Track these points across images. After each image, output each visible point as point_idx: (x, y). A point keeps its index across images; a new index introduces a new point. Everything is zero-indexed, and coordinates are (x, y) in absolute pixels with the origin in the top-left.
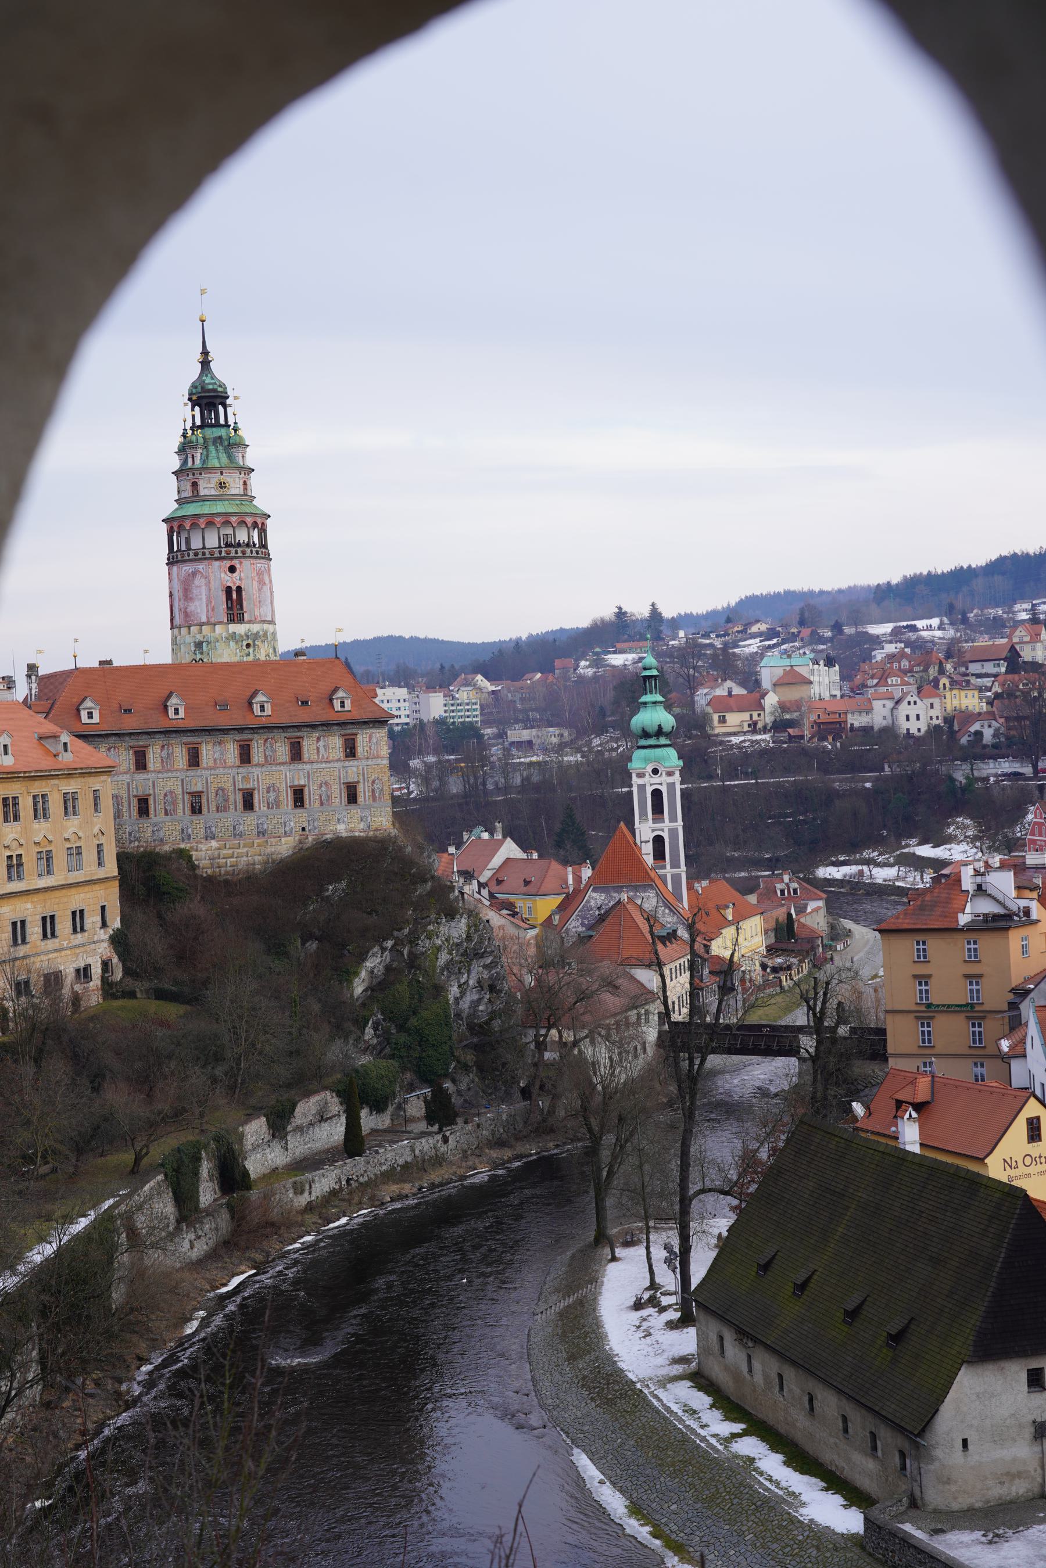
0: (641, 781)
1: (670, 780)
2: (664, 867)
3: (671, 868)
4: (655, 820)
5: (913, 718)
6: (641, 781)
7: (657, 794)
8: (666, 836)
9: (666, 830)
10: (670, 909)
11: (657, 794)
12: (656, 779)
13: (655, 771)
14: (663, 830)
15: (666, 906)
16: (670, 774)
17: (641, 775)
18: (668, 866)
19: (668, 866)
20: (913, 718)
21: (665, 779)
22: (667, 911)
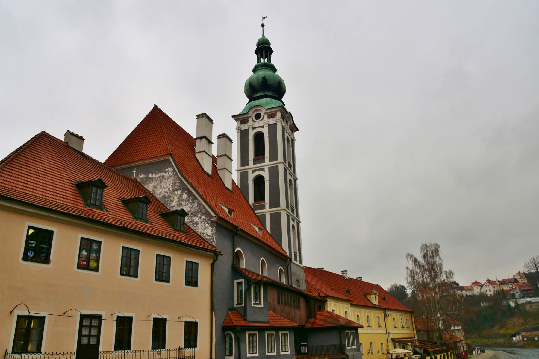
0: (244, 127)
1: (272, 121)
2: (264, 208)
3: (271, 207)
4: (255, 161)
5: (488, 291)
6: (244, 127)
7: (259, 137)
8: (266, 174)
9: (267, 169)
10: (190, 194)
11: (259, 137)
12: (259, 123)
13: (258, 116)
15: (184, 189)
18: (267, 206)
19: (267, 206)
20: (488, 291)
21: (267, 120)
22: (185, 196)
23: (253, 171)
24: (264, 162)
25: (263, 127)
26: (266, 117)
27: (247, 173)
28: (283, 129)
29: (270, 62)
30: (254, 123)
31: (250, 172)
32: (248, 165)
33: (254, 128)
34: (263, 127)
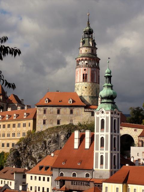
0: (98, 116)
6: (98, 116)
12: (103, 115)
13: (103, 112)
14: (104, 135)
16: (108, 113)
17: (98, 114)
23: (101, 135)
24: (104, 132)
25: (104, 117)
26: (105, 113)
27: (99, 135)
28: (112, 118)
29: (110, 83)
30: (101, 115)
31: (100, 135)
32: (99, 132)
33: (101, 117)
34: (104, 117)
